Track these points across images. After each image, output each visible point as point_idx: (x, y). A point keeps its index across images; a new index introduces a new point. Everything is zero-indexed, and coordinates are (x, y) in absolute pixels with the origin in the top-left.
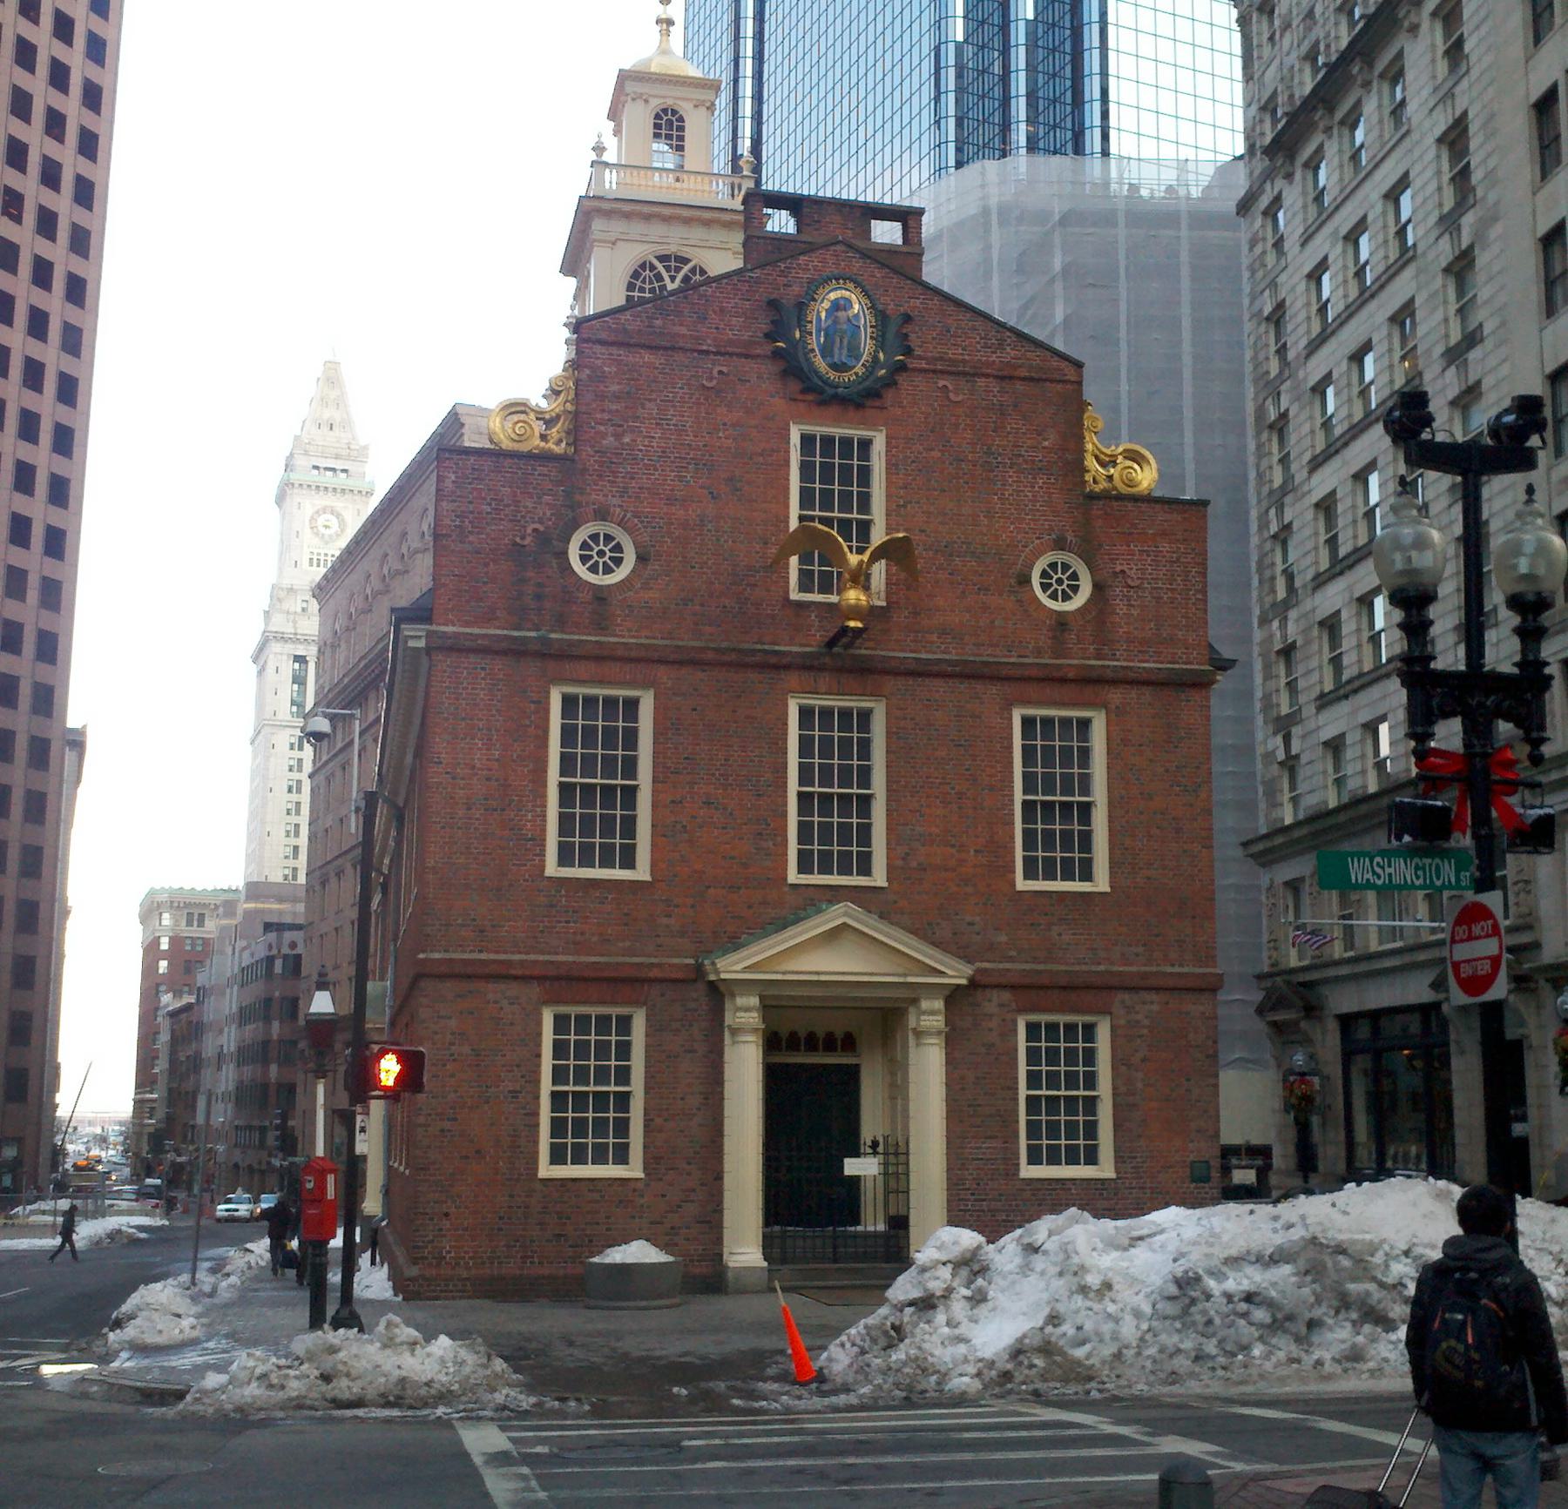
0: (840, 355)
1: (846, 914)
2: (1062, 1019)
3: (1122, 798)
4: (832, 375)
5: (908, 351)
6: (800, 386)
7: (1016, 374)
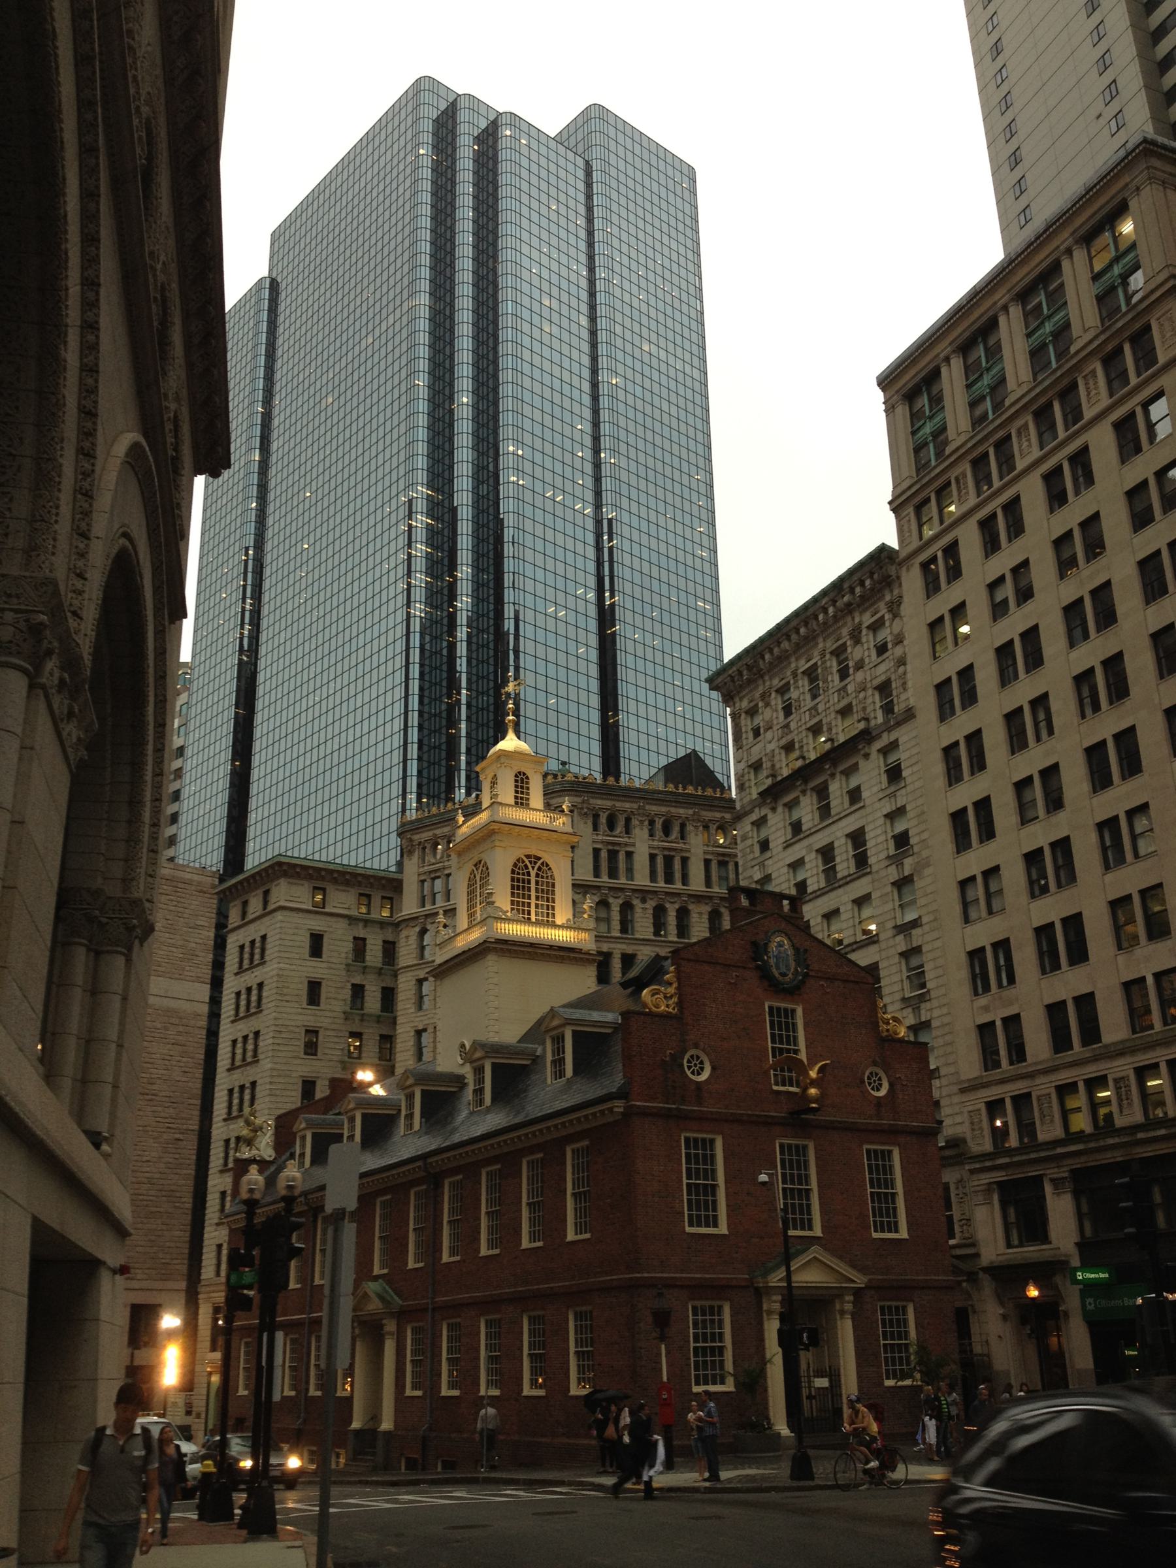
0: (783, 970)
1: (815, 1252)
4: (781, 978)
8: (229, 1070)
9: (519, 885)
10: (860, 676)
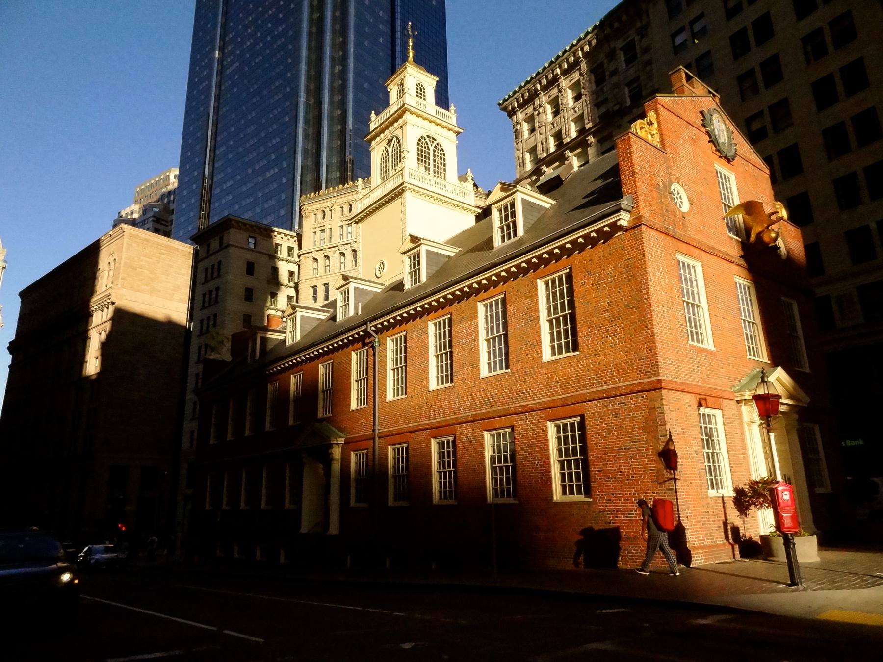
6: (714, 148)
8: (198, 336)
9: (423, 157)
10: (615, 79)
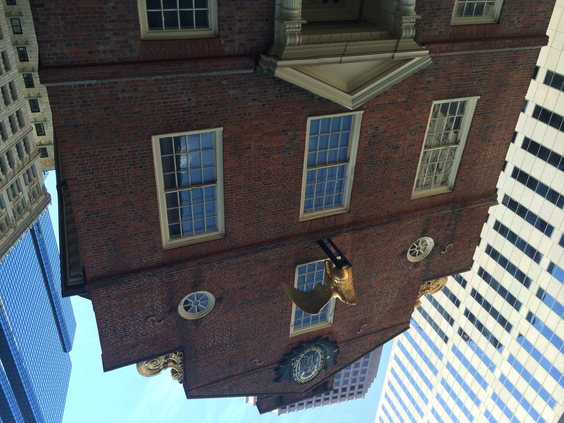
2: (180, 33)
3: (147, 199)
5: (277, 369)
7: (223, 381)
